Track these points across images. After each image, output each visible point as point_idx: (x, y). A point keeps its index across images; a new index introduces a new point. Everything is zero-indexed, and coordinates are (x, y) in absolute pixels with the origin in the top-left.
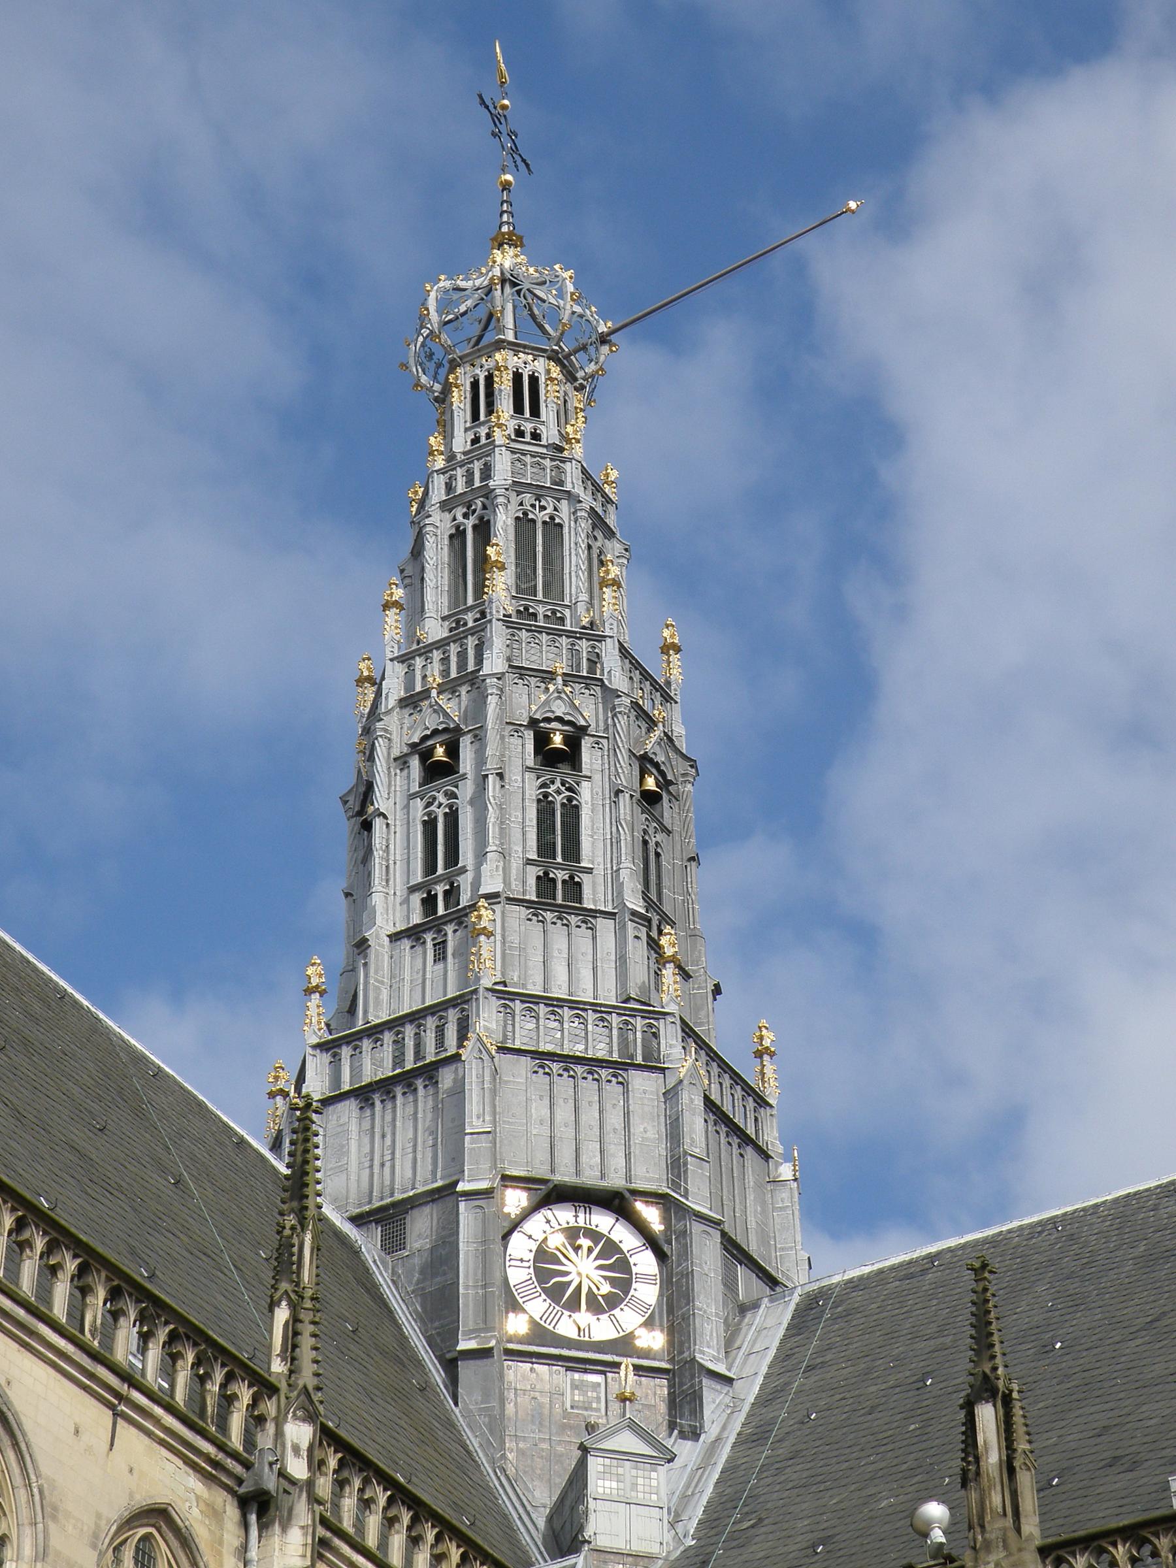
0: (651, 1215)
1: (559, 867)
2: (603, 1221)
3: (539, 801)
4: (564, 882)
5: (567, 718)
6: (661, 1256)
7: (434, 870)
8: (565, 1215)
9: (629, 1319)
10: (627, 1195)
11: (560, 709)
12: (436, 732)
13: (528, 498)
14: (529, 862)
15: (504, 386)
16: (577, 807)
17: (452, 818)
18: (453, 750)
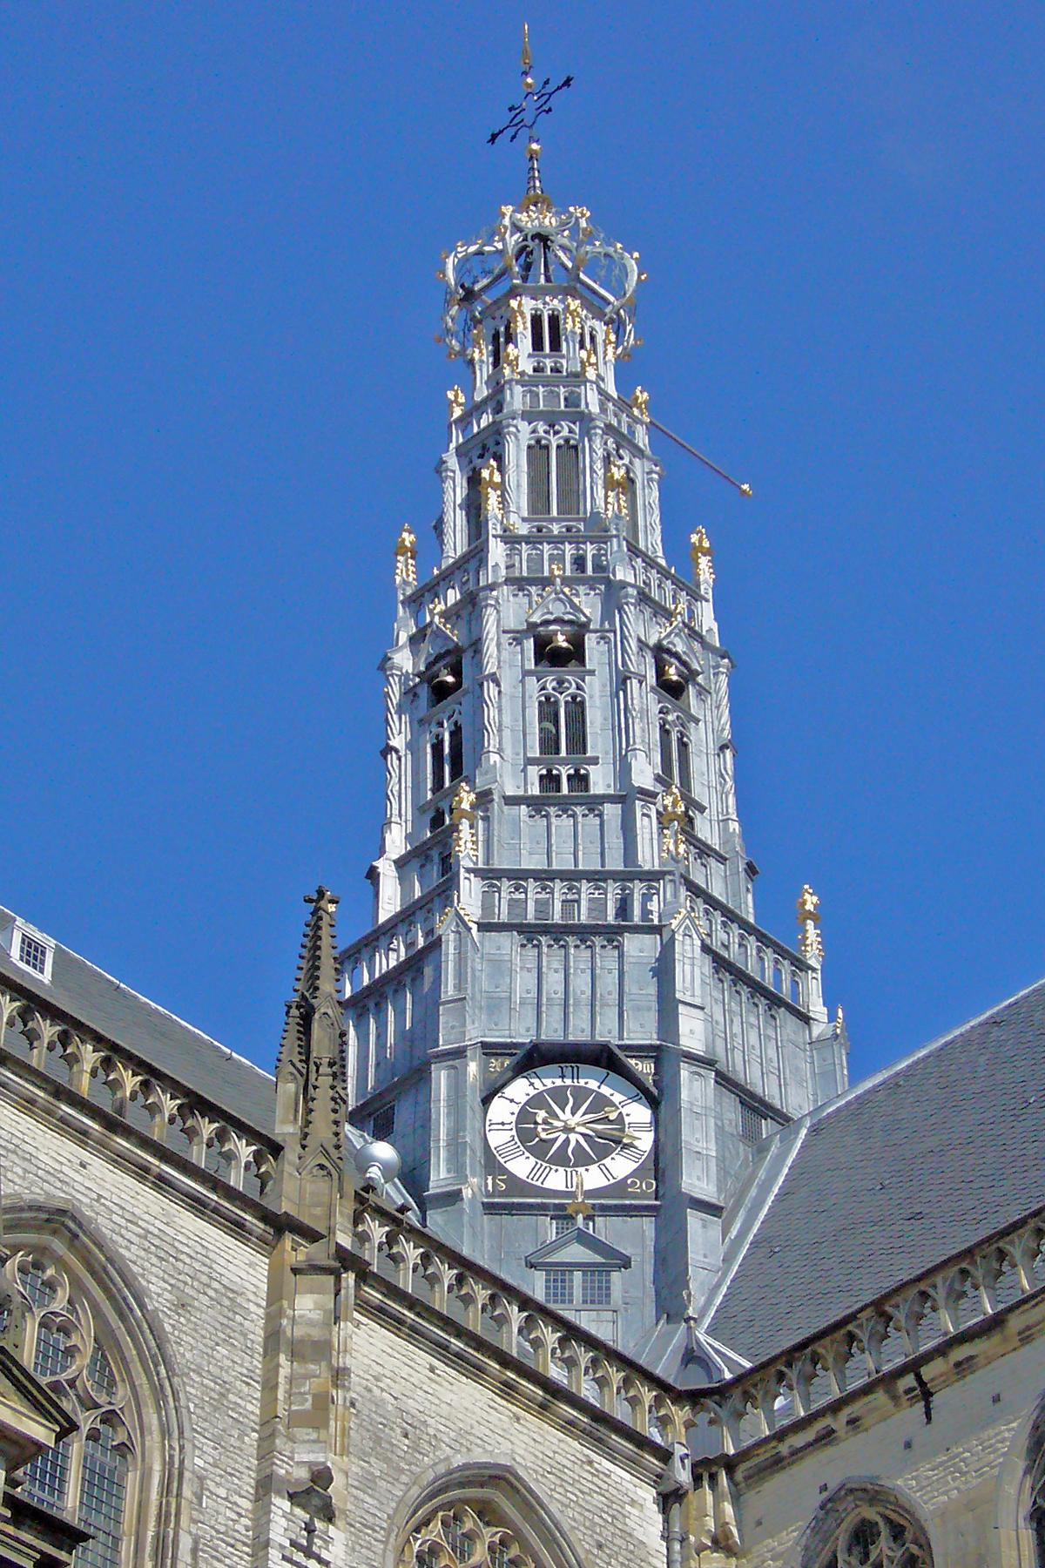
0: (644, 1068)
1: (564, 762)
3: (540, 703)
4: (569, 777)
5: (567, 617)
6: (654, 1103)
7: (442, 786)
9: (621, 1166)
11: (558, 610)
13: (541, 427)
14: (530, 761)
15: (524, 330)
16: (582, 703)
18: (457, 671)
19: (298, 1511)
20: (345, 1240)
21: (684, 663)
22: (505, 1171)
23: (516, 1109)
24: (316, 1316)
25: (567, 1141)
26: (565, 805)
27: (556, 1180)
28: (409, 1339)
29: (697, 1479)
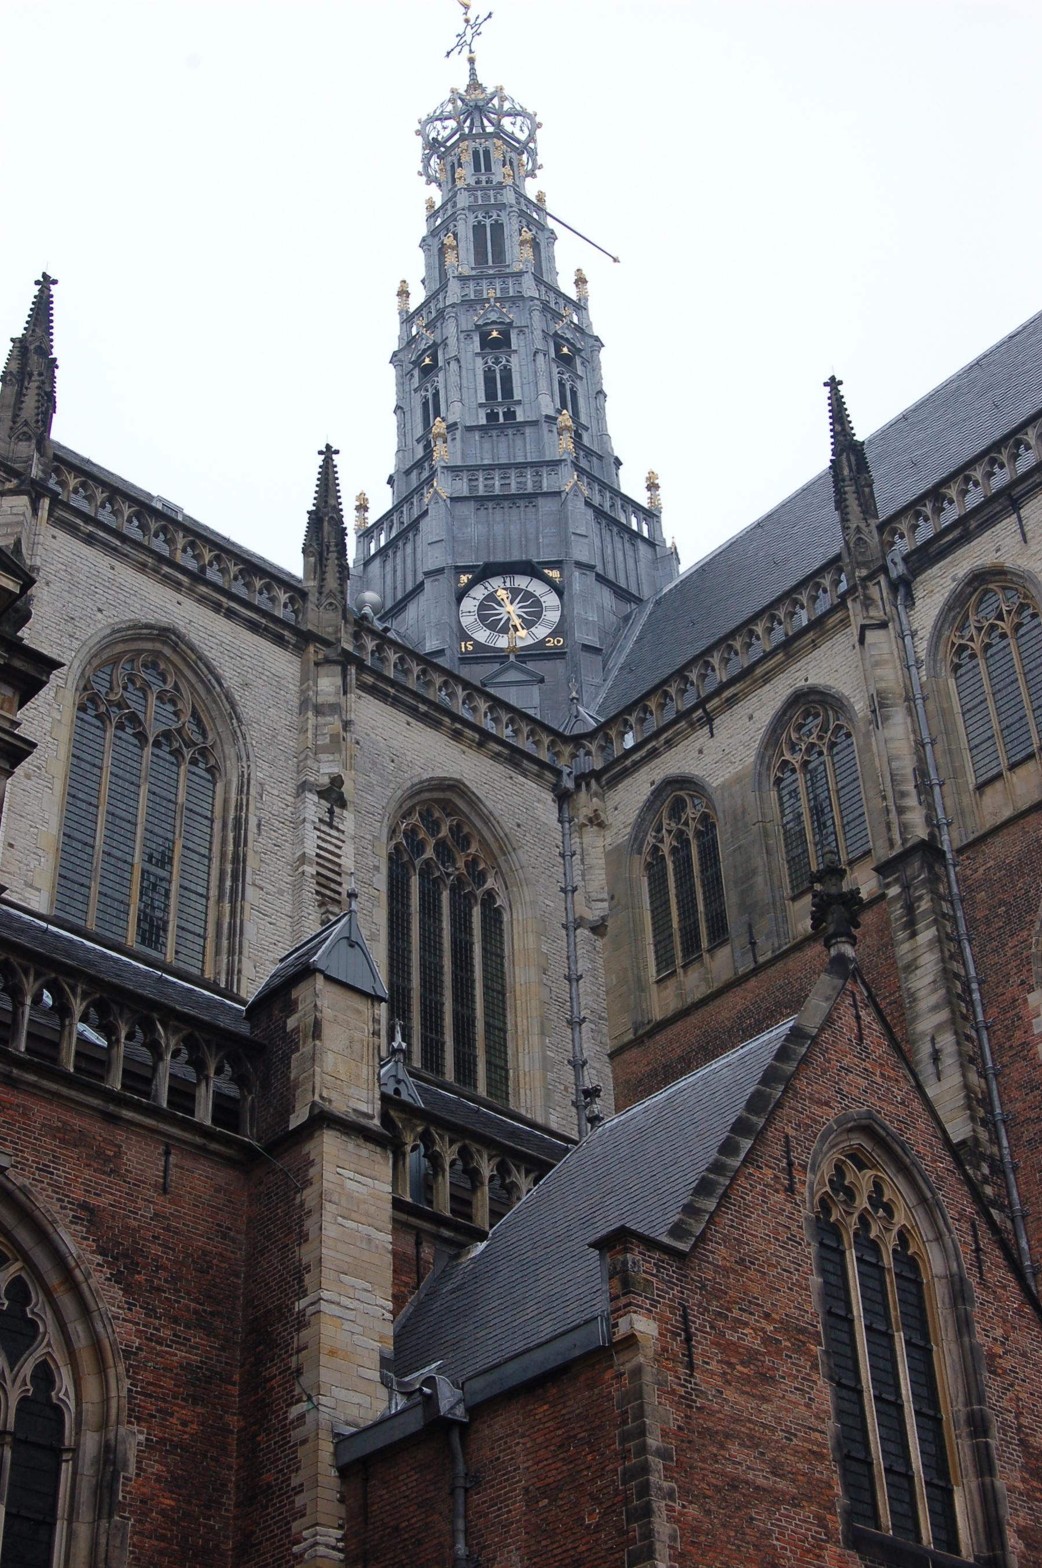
0: (554, 574)
1: (501, 404)
2: (522, 582)
6: (560, 594)
8: (497, 585)
10: (539, 567)
11: (493, 317)
12: (424, 351)
15: (467, 158)
17: (436, 395)
18: (435, 358)
19: (323, 802)
20: (350, 648)
21: (572, 345)
22: (471, 639)
23: (477, 603)
24: (331, 689)
25: (509, 619)
26: (502, 428)
27: (502, 642)
28: (392, 705)
29: (578, 786)
